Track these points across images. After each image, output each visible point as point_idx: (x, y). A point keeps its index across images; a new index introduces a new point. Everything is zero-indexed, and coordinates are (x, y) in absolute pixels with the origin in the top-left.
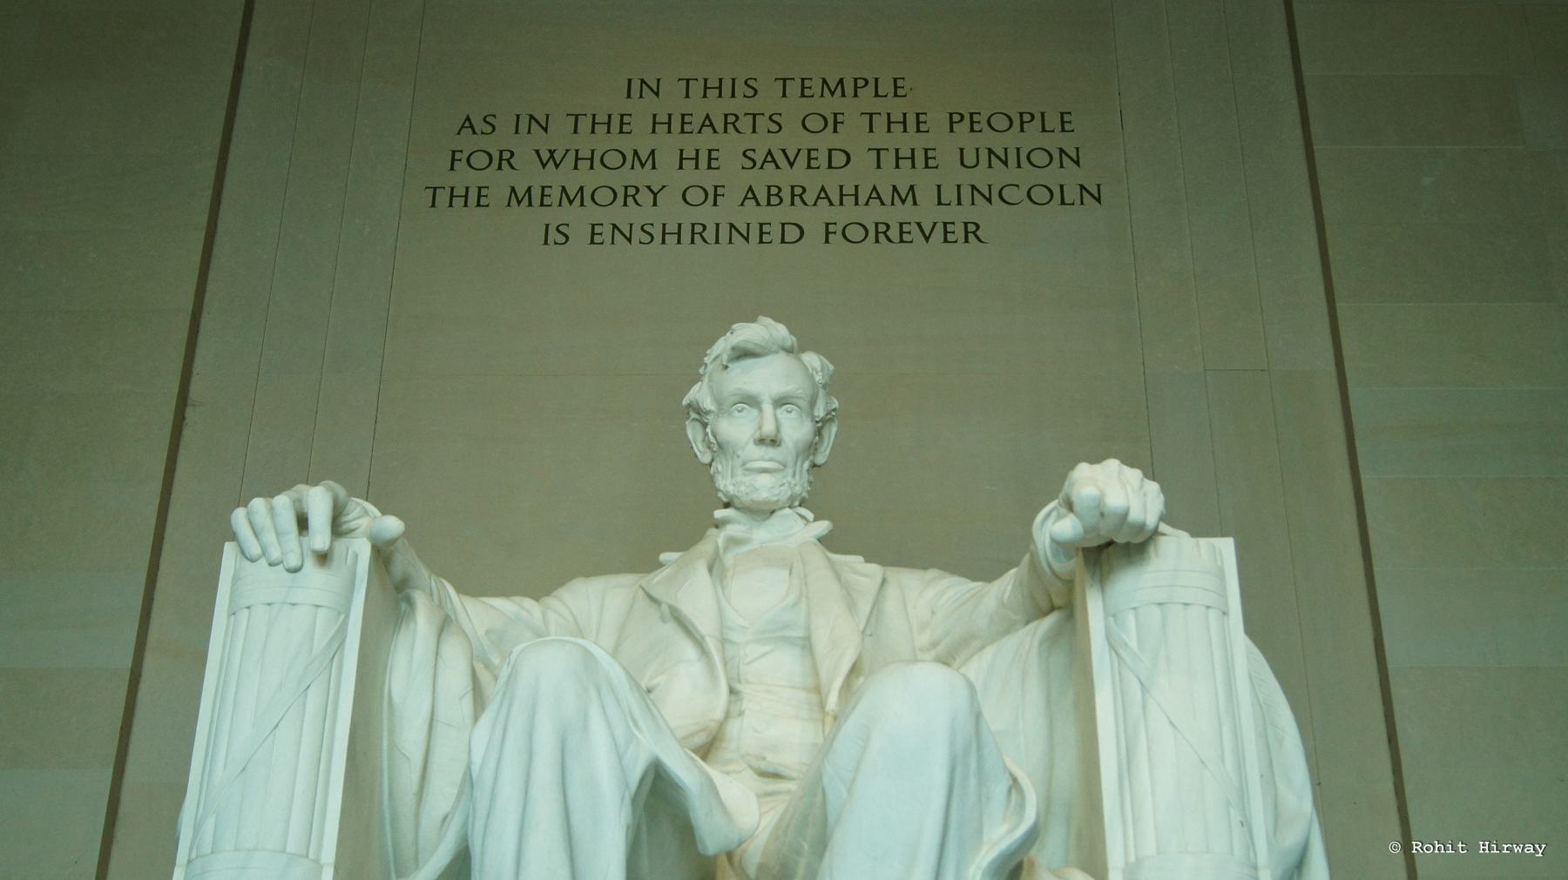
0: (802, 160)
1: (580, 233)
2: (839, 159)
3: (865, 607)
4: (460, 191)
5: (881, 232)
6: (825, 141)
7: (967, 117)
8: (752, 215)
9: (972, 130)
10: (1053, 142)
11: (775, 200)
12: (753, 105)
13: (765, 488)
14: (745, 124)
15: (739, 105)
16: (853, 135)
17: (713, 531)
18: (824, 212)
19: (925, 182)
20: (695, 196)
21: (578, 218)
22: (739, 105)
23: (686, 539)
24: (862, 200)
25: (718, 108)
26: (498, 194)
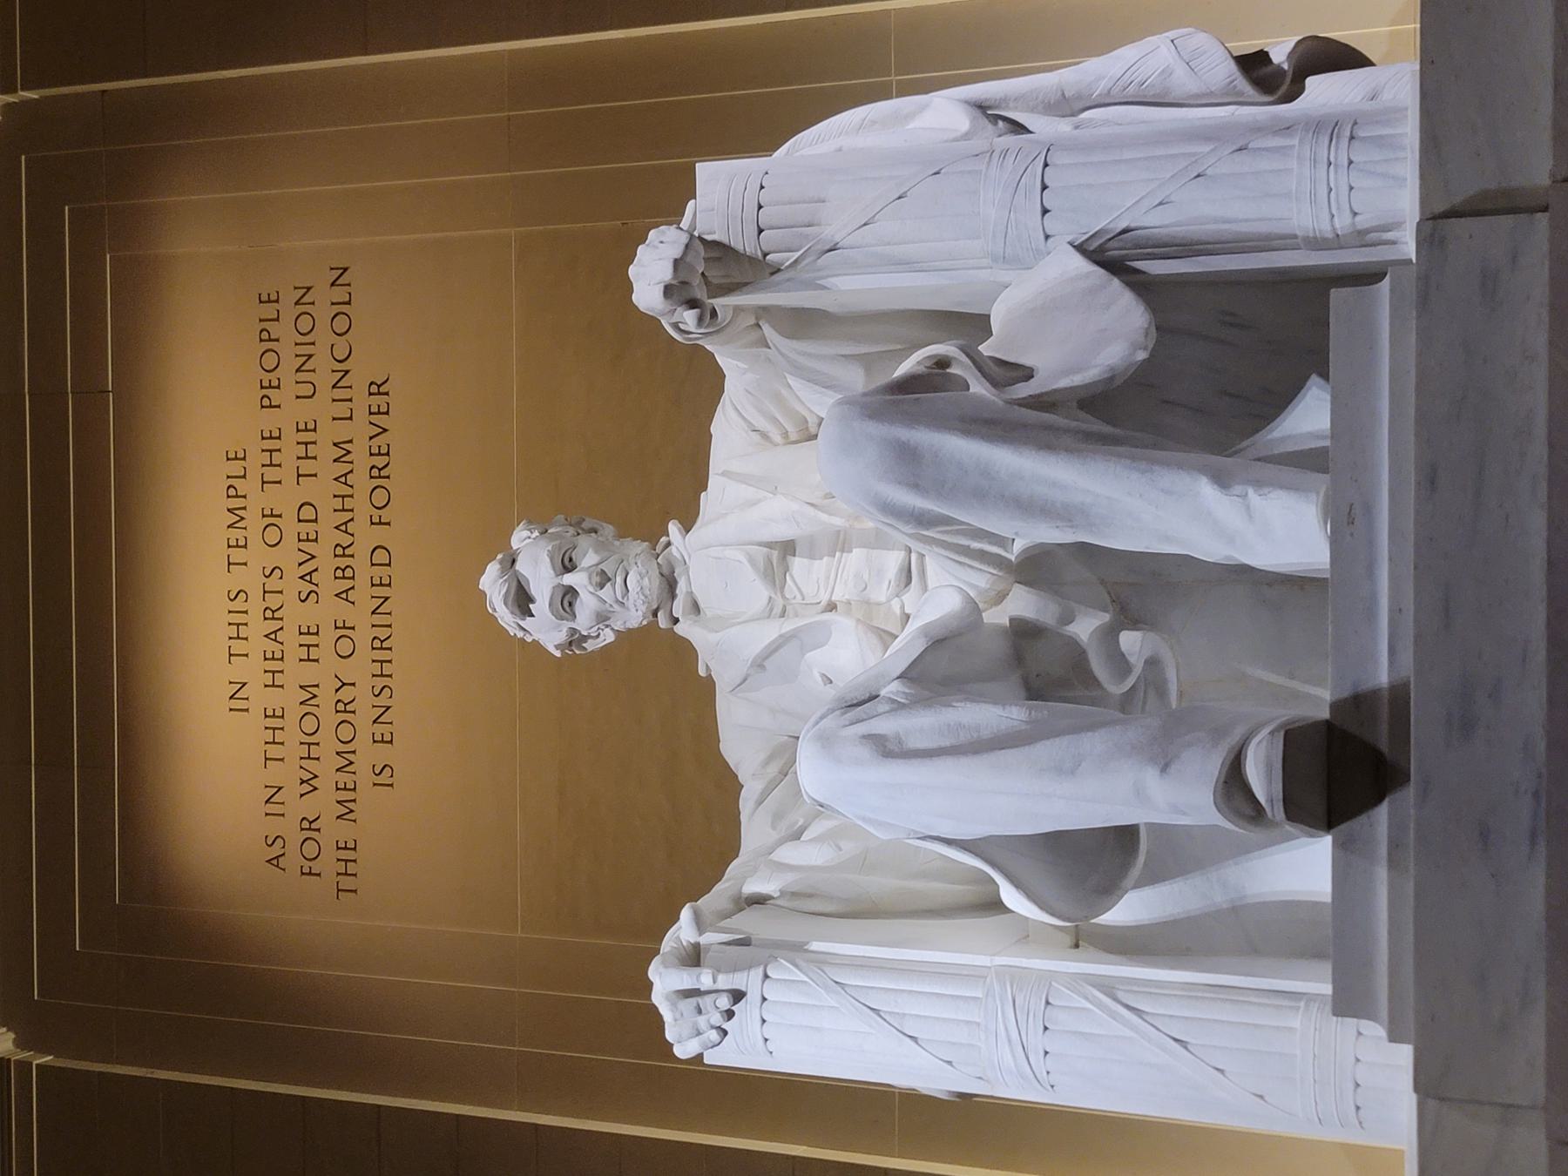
0: (310, 547)
1: (383, 754)
2: (308, 513)
3: (748, 492)
4: (341, 867)
7: (265, 392)
9: (278, 387)
10: (288, 311)
11: (349, 573)
12: (256, 594)
13: (640, 582)
14: (273, 601)
17: (679, 629)
18: (360, 526)
19: (328, 433)
20: (345, 647)
21: (367, 756)
22: (256, 606)
23: (685, 651)
24: (349, 491)
26: (345, 832)
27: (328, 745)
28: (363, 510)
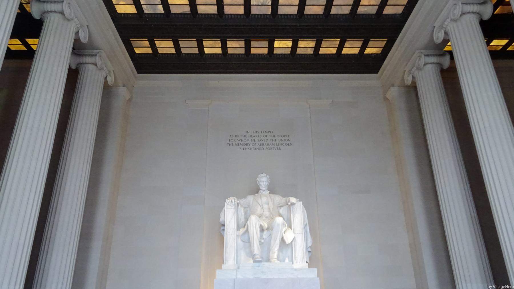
5: (271, 148)
6: (266, 138)
8: (259, 147)
10: (288, 138)
13: (264, 189)
15: (257, 134)
16: (268, 138)
19: (275, 143)
21: (242, 147)
22: (257, 134)
25: (255, 134)
27: (243, 142)
28: (268, 146)
